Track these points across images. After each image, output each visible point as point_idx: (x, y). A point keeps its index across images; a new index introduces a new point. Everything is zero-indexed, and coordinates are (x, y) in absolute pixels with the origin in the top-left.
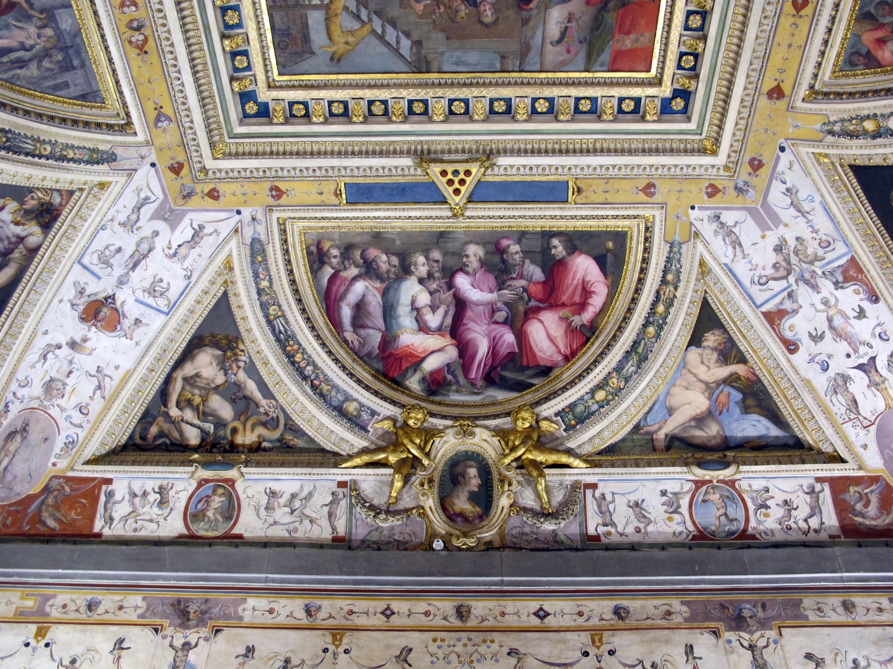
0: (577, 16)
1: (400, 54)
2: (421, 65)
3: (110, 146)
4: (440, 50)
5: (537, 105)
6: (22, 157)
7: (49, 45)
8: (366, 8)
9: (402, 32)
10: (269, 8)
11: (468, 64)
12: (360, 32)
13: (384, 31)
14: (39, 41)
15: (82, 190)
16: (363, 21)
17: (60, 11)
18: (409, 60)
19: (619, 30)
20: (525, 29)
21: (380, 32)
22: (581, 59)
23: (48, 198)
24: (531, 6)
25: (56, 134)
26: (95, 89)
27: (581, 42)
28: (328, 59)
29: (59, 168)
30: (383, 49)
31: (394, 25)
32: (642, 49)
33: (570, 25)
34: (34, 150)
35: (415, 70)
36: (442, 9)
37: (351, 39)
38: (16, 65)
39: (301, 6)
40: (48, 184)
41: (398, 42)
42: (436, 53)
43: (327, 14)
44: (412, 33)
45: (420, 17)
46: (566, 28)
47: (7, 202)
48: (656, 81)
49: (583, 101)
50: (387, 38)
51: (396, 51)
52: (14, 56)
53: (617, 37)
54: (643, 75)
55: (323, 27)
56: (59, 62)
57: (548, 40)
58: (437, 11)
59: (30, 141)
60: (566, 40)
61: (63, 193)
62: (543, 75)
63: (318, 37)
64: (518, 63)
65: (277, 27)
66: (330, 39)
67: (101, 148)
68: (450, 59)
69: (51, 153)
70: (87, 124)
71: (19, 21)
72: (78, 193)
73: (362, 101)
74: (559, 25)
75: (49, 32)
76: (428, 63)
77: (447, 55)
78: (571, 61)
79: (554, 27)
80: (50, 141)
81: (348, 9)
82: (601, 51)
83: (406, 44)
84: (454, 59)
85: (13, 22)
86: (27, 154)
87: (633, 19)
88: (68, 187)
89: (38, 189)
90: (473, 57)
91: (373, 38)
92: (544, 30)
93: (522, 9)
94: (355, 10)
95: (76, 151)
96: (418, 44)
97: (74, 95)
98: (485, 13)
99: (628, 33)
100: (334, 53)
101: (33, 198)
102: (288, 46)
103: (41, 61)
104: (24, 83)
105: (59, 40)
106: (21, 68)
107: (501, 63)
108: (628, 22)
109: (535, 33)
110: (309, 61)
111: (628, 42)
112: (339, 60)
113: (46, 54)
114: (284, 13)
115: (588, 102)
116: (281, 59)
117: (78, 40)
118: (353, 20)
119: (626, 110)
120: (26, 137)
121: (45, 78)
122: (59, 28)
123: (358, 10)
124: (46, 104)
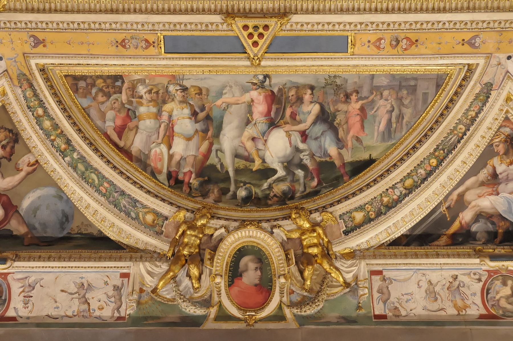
3: (479, 85)
6: (459, 146)
7: (394, 96)
14: (390, 101)
15: (507, 112)
17: (374, 82)
23: (503, 136)
25: (453, 118)
26: (436, 77)
29: (479, 125)
34: (458, 136)
38: (400, 119)
40: (492, 132)
47: (491, 163)
52: (394, 120)
56: (408, 94)
59: (451, 136)
61: (504, 124)
67: (477, 91)
69: (465, 126)
70: (456, 93)
71: (373, 108)
72: (509, 115)
75: (386, 93)
80: (456, 123)
85: (373, 112)
86: (459, 142)
88: (501, 118)
89: (492, 140)
95: (472, 109)
97: (434, 91)
101: (497, 146)
103: (403, 104)
104: (414, 120)
105: (393, 89)
106: (403, 118)
113: (400, 100)
117: (397, 77)
120: (446, 138)
121: (415, 107)
122: (385, 86)
124: (433, 113)
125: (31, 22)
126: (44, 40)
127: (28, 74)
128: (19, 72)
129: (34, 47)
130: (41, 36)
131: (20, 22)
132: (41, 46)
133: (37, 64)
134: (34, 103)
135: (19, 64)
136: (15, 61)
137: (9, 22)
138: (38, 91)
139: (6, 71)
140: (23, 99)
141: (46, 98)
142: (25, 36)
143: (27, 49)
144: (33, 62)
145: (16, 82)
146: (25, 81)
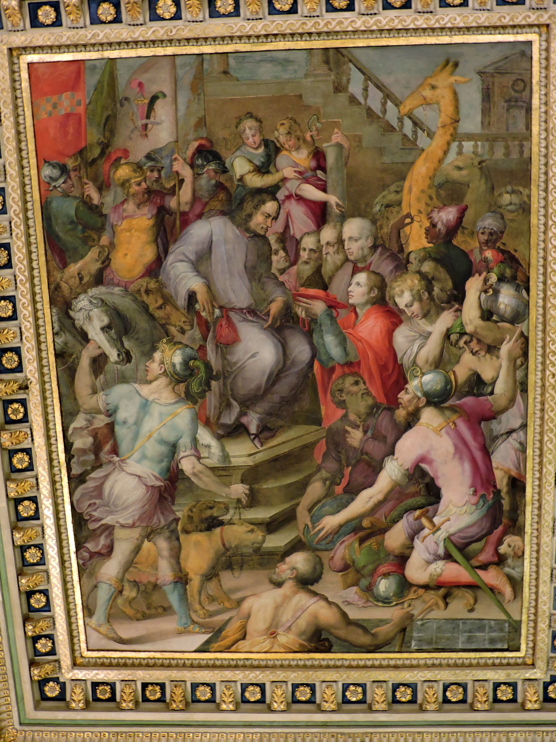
0: (137, 133)
1: (363, 73)
2: (335, 59)
4: (309, 80)
5: (173, 9)
8: (405, 136)
9: (360, 104)
10: (529, 137)
11: (272, 61)
12: (416, 102)
13: (384, 104)
16: (410, 118)
18: (351, 65)
19: (80, 119)
20: (201, 114)
21: (389, 103)
22: (122, 78)
24: (196, 144)
27: (126, 99)
28: (460, 65)
30: (387, 80)
31: (370, 112)
32: (45, 94)
33: (144, 121)
35: (342, 50)
36: (308, 138)
37: (427, 93)
39: (487, 140)
41: (366, 89)
42: (316, 76)
43: (455, 128)
44: (347, 103)
45: (336, 125)
46: (148, 117)
48: (15, 53)
49: (110, 18)
50: (381, 95)
51: (368, 77)
53: (81, 110)
54: (34, 58)
55: (464, 110)
57: (169, 99)
58: (315, 133)
60: (147, 101)
62: (170, 51)
63: (471, 96)
64: (205, 66)
65: (523, 112)
66: (455, 94)
68: (296, 67)
73: (420, 8)
74: (158, 120)
76: (327, 62)
77: (301, 73)
78: (135, 72)
79: (163, 118)
81: (428, 135)
82: (98, 88)
83: (356, 86)
84: (290, 68)
87: (66, 133)
90: (266, 72)
91: (398, 95)
92: (176, 110)
93: (207, 139)
94: (420, 132)
96: (339, 88)
98: (253, 132)
99: (68, 116)
100: (452, 74)
102: (513, 85)
107: (228, 64)
108: (71, 130)
109: (188, 107)
110: (487, 61)
111: (66, 102)
112: (447, 62)
114: (512, 130)
115: (103, 18)
116: (525, 65)
118: (423, 119)
119: (47, 8)
123: (415, 133)
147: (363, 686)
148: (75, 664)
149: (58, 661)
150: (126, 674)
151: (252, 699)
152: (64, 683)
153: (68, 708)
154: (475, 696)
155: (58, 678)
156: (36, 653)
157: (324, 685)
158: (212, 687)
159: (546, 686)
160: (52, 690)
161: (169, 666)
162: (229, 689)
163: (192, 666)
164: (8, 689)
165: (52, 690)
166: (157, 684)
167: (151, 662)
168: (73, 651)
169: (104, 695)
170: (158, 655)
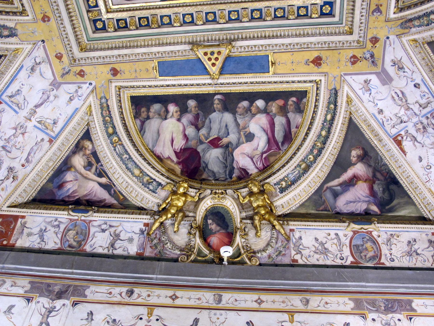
125: (361, 13)
126: (376, 5)
127: (401, 21)
128: (399, 27)
129: (381, 12)
130: (373, 7)
131: (360, 20)
132: (381, 8)
133: (394, 13)
134: (425, 20)
135: (393, 26)
136: (391, 28)
137: (360, 27)
138: (416, 15)
139: (397, 36)
140: (420, 28)
141: (422, 10)
142: (372, 18)
143: (382, 18)
144: (392, 16)
145: (407, 31)
146: (407, 24)
147: (238, 11)
148: (108, 12)
149: (100, 10)
150: (130, 14)
151: (188, 21)
152: (104, 21)
153: (107, 32)
154: (288, 12)
155: (101, 19)
156: (90, 6)
157: (220, 11)
158: (169, 17)
159: (322, 7)
160: (99, 25)
161: (150, 9)
162: (177, 17)
163: (160, 8)
164: (79, 23)
165: (99, 25)
166: (145, 18)
167: (141, 8)
168: (106, 6)
169: (122, 25)
170: (144, 4)
